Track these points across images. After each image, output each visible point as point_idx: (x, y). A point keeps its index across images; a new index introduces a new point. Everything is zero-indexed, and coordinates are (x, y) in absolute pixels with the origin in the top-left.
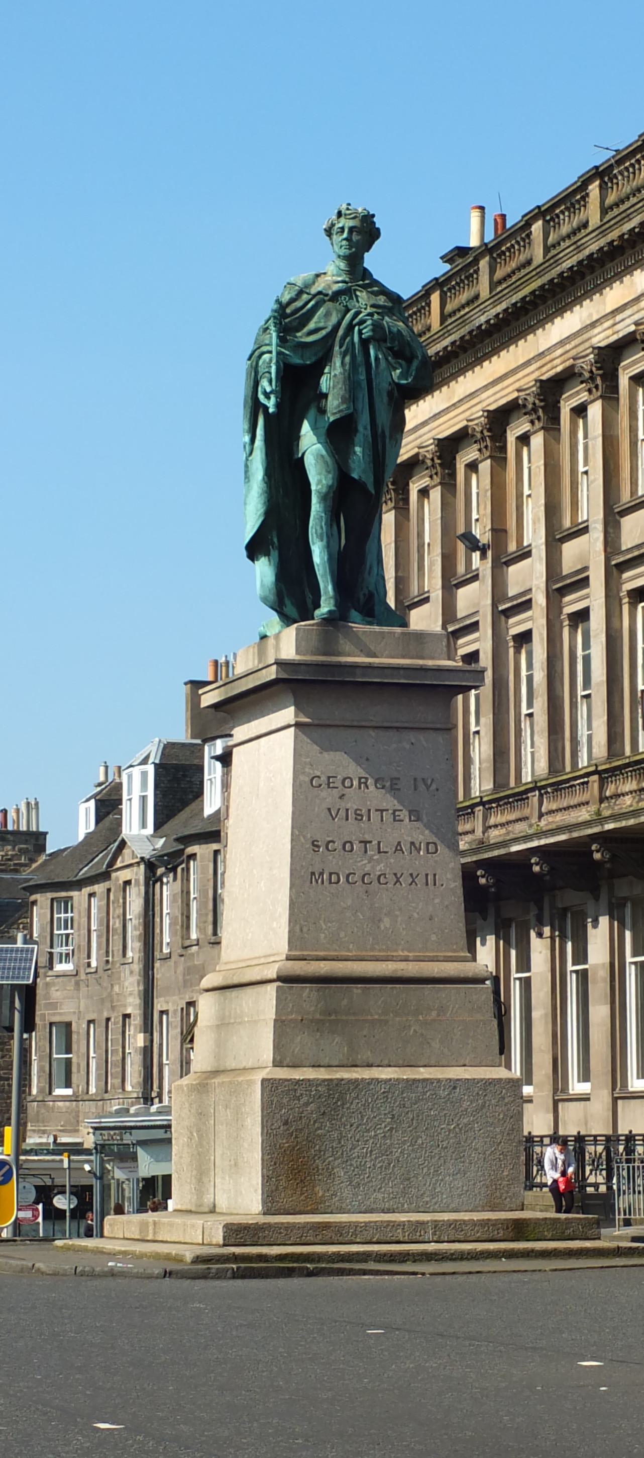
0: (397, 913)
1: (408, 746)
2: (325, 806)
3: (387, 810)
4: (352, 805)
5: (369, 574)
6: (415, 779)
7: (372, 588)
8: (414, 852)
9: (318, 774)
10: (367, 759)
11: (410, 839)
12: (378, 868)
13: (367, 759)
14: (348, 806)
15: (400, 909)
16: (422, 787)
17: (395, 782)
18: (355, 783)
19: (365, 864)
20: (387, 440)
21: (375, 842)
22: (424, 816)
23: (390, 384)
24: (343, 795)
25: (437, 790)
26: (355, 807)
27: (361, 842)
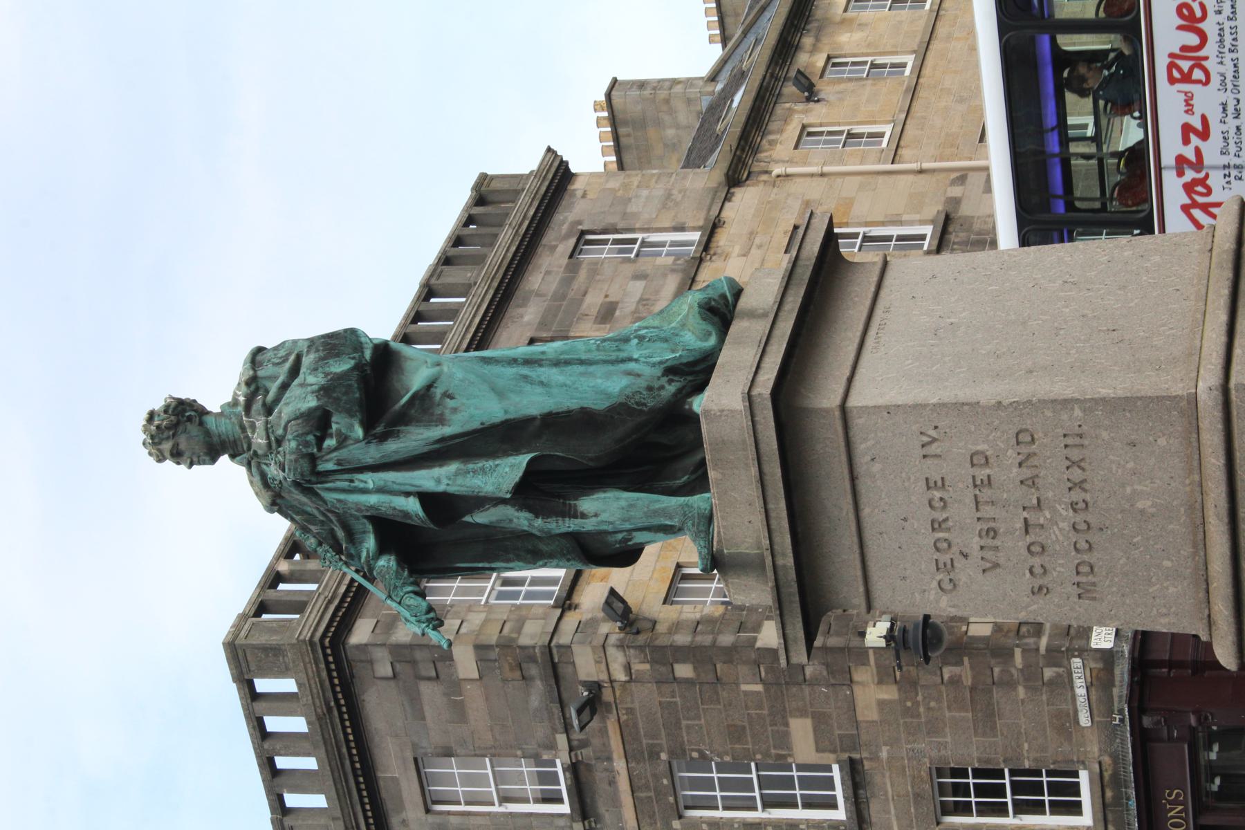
0: (1129, 490)
1: (876, 467)
2: (980, 576)
3: (976, 496)
4: (976, 542)
5: (639, 375)
6: (925, 456)
7: (658, 371)
8: (1034, 461)
9: (935, 584)
10: (905, 520)
11: (1015, 470)
12: (1064, 513)
13: (905, 520)
14: (977, 547)
15: (1123, 485)
16: (934, 449)
17: (932, 484)
18: (941, 535)
19: (1060, 530)
20: (447, 431)
21: (1025, 514)
22: (979, 448)
23: (369, 442)
24: (961, 553)
25: (936, 427)
26: (977, 538)
27: (1027, 532)
